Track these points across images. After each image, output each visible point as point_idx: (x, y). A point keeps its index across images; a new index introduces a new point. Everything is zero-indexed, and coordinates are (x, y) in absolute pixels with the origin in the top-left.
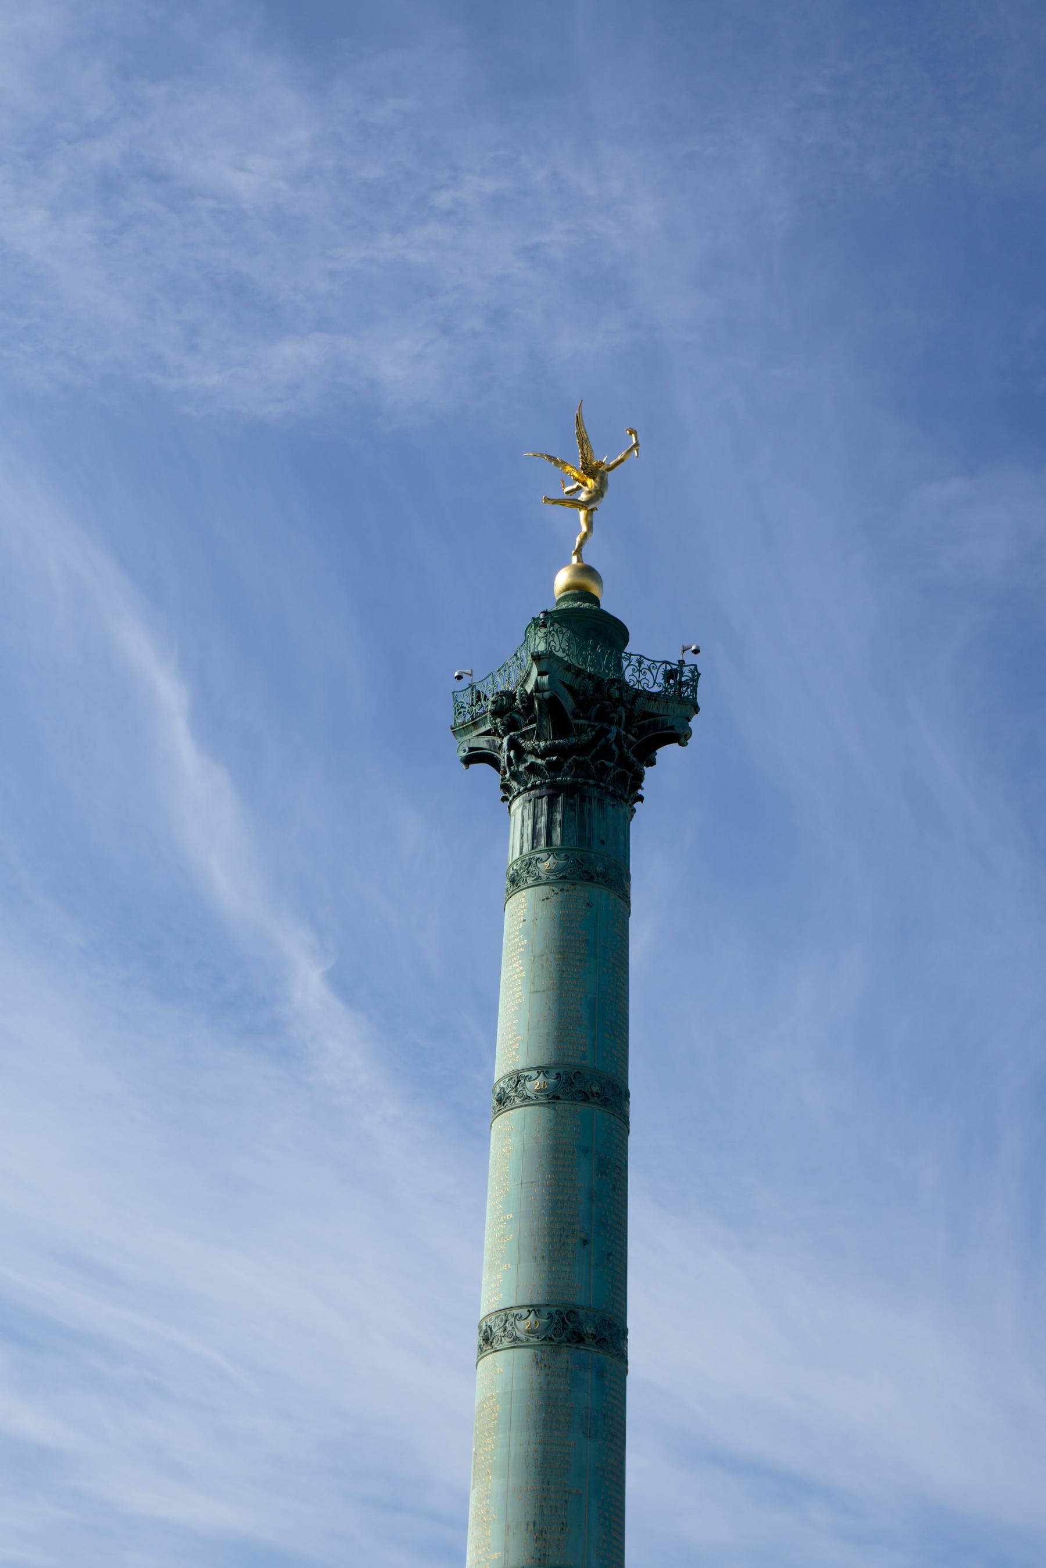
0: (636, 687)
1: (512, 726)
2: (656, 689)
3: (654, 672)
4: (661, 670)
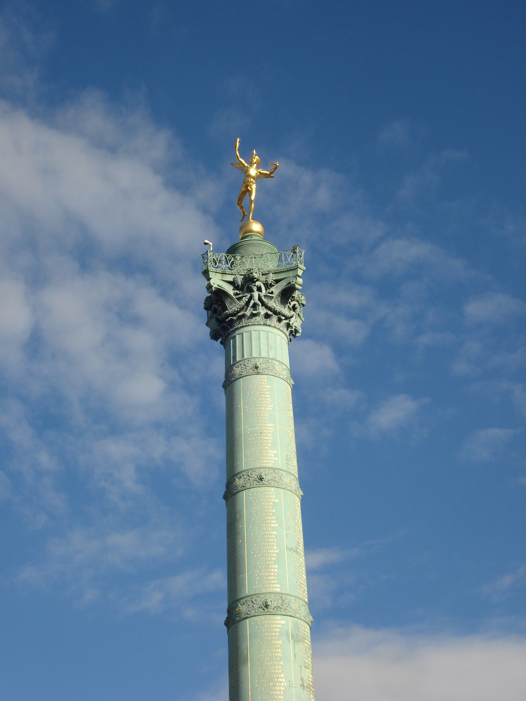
1: (215, 311)
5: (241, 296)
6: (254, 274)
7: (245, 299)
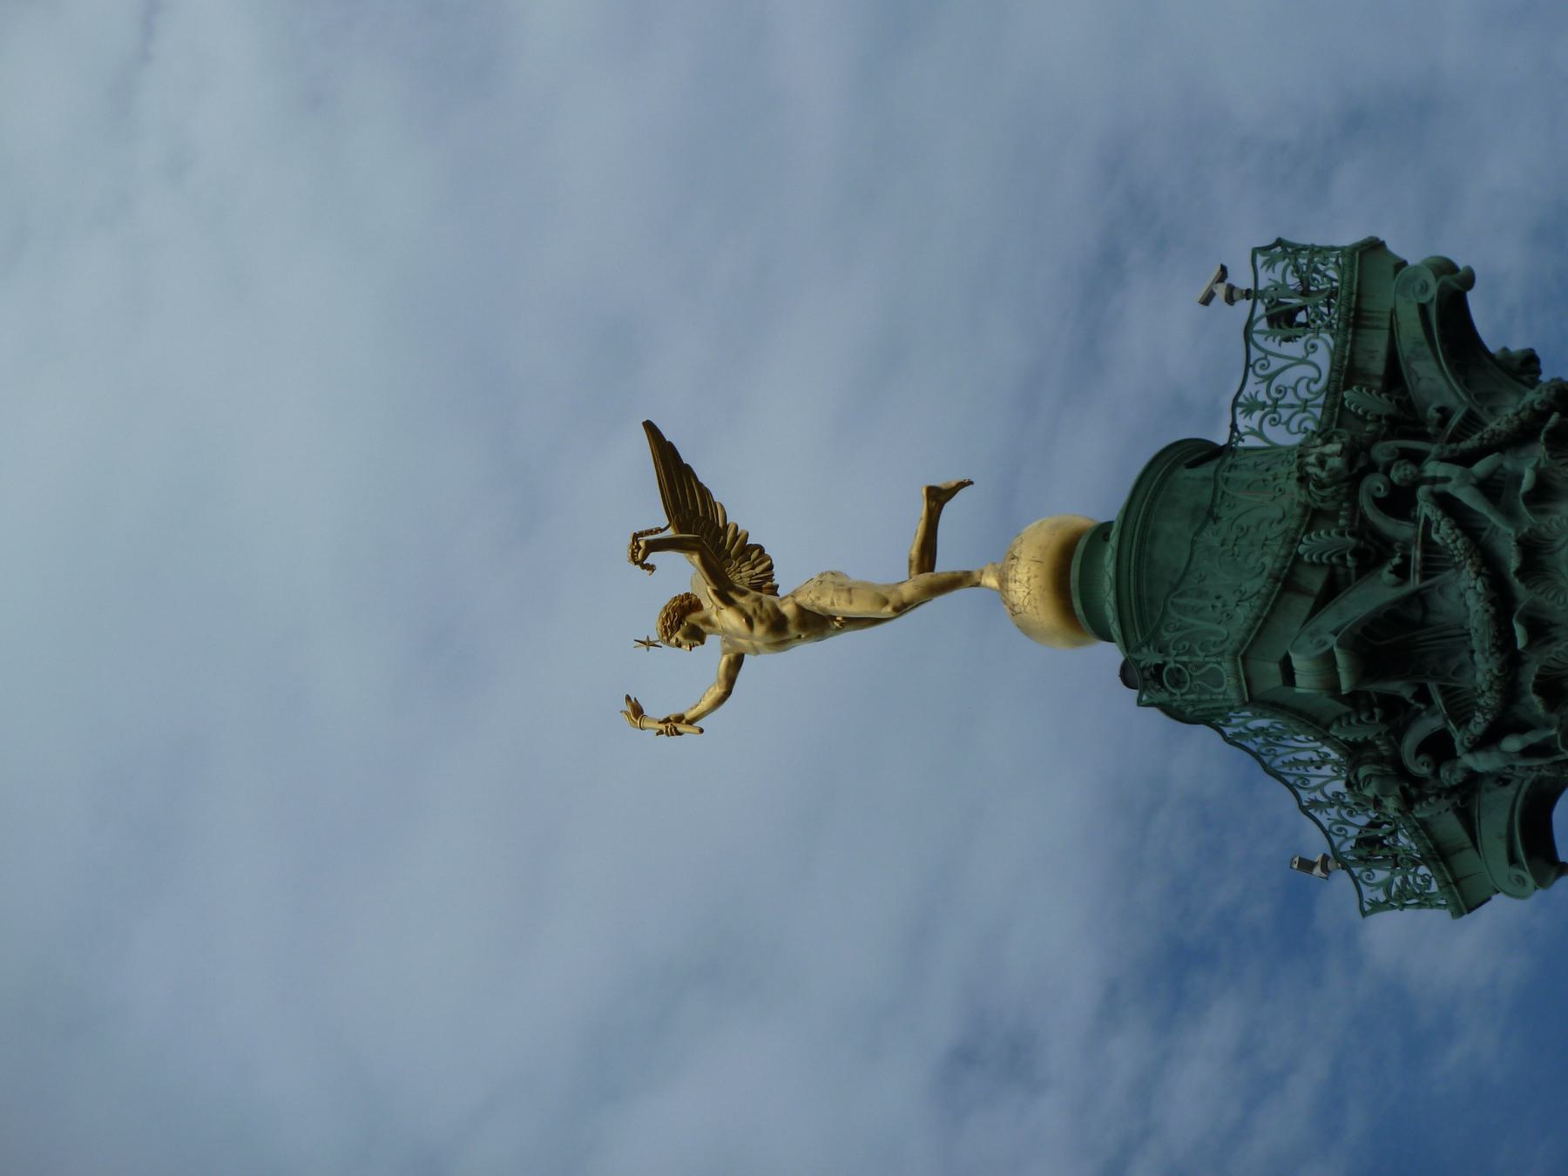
0: (1318, 412)
1: (1439, 748)
2: (1322, 358)
3: (1276, 364)
4: (1271, 345)
5: (1416, 554)
6: (1335, 447)
7: (1444, 533)
